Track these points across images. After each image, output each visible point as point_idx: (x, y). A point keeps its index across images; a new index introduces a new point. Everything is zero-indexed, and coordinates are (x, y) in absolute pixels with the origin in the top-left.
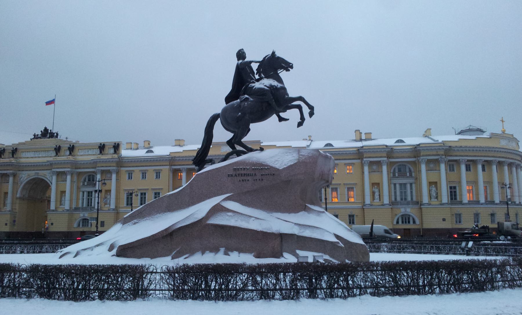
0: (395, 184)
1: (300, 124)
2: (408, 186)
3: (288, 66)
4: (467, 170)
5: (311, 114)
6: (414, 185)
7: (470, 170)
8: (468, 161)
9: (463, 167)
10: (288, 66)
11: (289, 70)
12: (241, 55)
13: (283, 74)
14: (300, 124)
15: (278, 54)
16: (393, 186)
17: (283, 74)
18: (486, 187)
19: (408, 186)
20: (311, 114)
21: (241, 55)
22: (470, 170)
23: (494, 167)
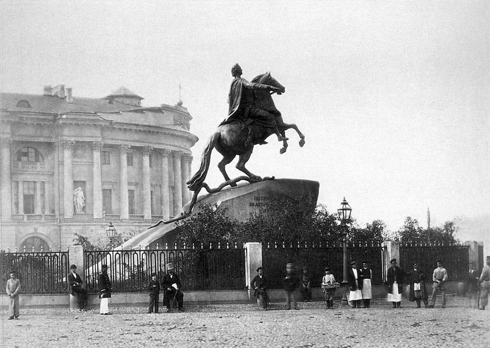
0: (17, 182)
1: (283, 151)
2: (38, 186)
3: (280, 90)
4: (128, 165)
5: (302, 143)
6: (47, 186)
7: (132, 165)
8: (133, 147)
9: (124, 157)
10: (280, 90)
11: (281, 94)
12: (237, 71)
13: (275, 97)
14: (283, 151)
15: (273, 76)
16: (13, 184)
17: (275, 97)
18: (131, 192)
19: (38, 186)
20: (302, 143)
21: (237, 71)
22: (132, 165)
23: (165, 161)
